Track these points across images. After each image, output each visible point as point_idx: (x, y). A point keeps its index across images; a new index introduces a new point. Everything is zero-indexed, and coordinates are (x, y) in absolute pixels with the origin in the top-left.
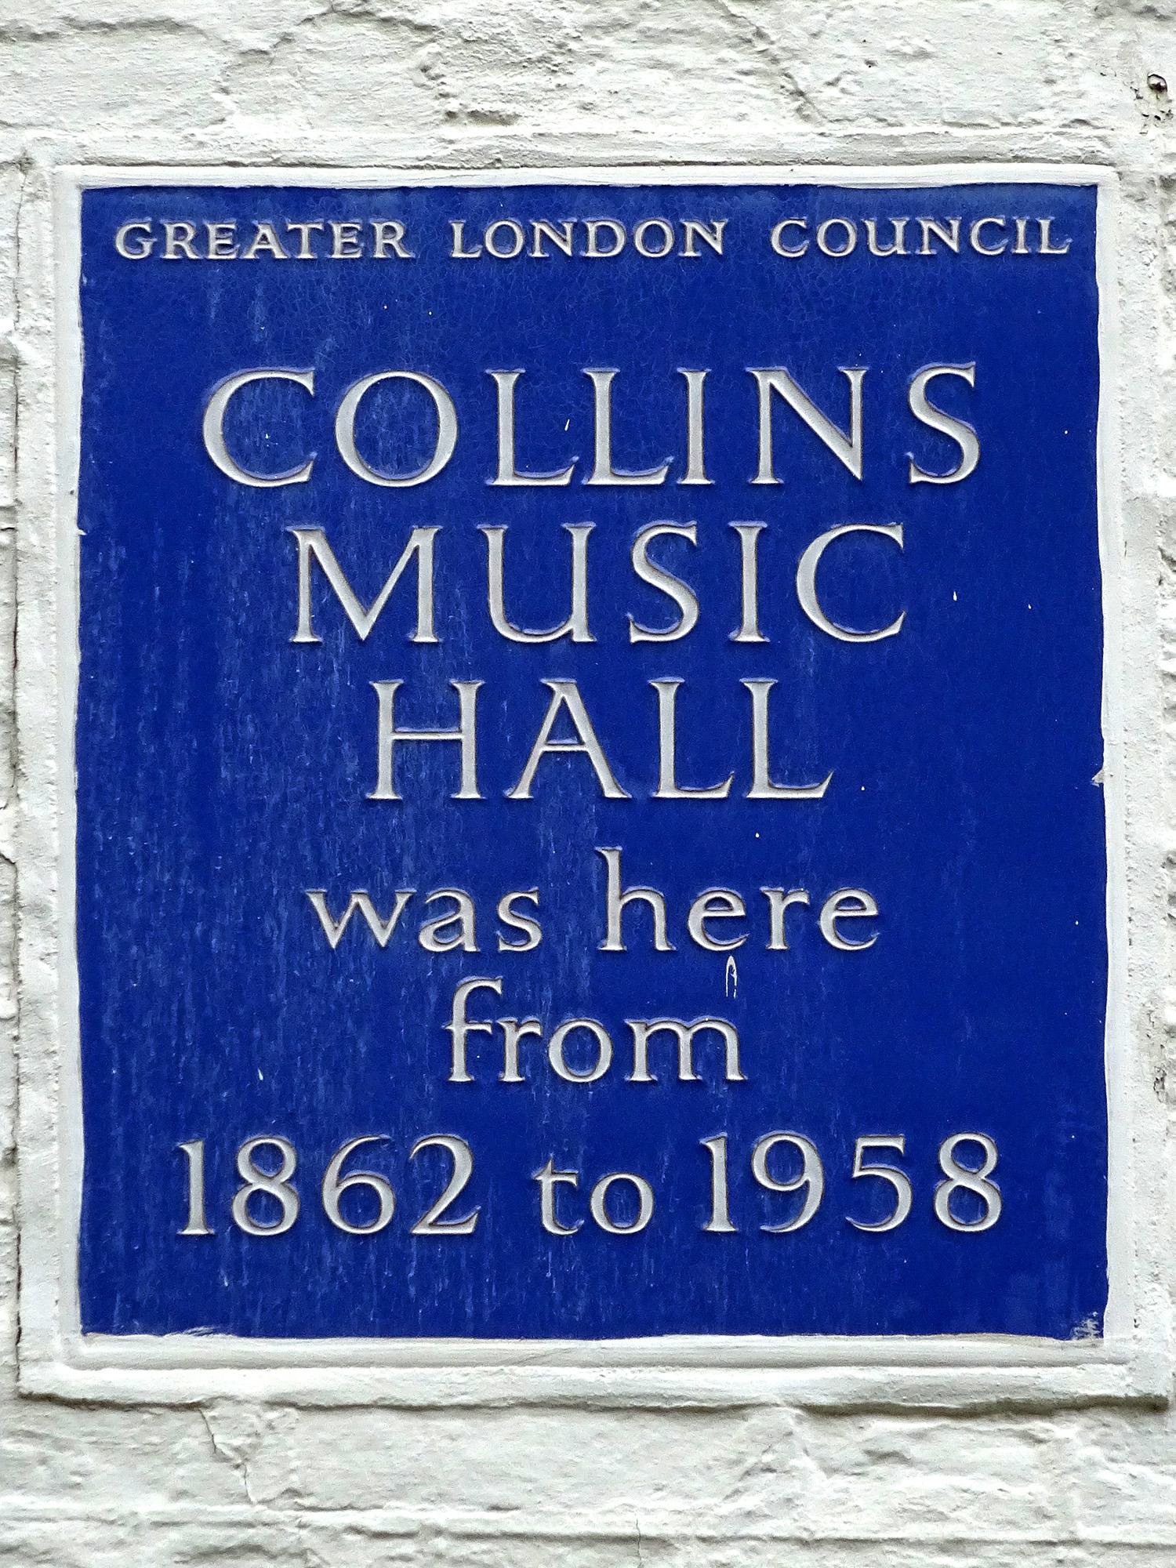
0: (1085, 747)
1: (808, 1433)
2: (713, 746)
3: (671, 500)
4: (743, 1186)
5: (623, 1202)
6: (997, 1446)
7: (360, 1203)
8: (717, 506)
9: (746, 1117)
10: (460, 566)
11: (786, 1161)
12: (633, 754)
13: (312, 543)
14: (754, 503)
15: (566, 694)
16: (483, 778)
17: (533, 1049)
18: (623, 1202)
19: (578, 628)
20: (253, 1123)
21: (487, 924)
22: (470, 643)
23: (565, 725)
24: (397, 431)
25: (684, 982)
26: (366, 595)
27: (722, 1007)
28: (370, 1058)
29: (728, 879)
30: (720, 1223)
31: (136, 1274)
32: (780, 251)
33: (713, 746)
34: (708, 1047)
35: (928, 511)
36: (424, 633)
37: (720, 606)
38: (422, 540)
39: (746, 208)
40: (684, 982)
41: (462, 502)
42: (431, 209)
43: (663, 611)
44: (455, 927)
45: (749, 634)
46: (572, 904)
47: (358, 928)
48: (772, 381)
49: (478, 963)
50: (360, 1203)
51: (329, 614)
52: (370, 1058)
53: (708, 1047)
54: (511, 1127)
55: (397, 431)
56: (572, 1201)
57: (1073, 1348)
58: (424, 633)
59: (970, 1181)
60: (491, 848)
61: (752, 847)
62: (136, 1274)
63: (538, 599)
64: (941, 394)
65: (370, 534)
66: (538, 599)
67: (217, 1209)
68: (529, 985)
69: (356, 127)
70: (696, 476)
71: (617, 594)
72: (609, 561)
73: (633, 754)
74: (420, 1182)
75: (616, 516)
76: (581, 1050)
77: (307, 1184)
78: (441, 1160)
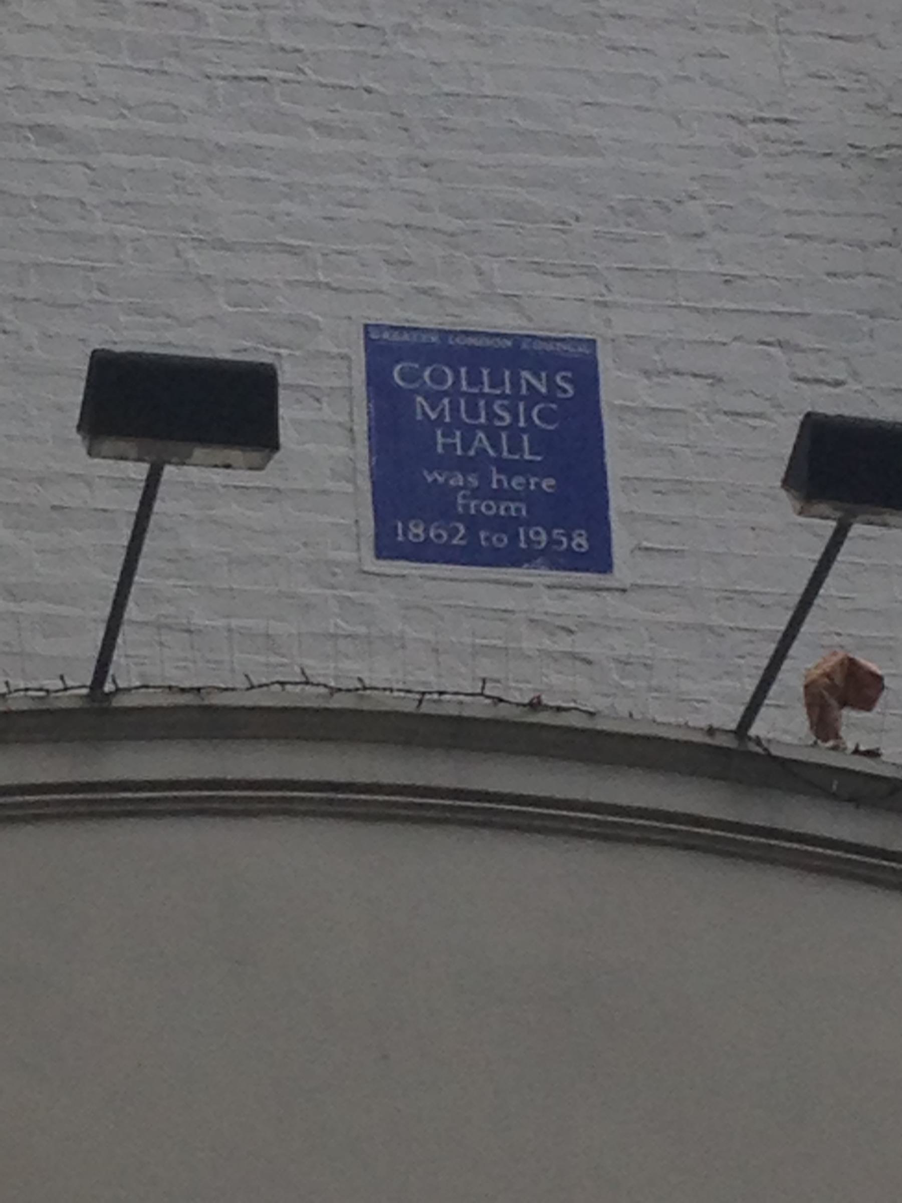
0: (601, 453)
1: (547, 591)
2: (515, 447)
3: (503, 396)
4: (528, 540)
5: (500, 540)
6: (588, 598)
7: (439, 536)
8: (516, 397)
9: (528, 524)
10: (454, 409)
11: (537, 533)
12: (496, 446)
13: (419, 399)
14: (523, 398)
15: (481, 435)
16: (463, 448)
17: (477, 508)
18: (500, 540)
19: (483, 420)
20: (413, 517)
21: (465, 480)
22: (457, 422)
23: (481, 441)
24: (438, 378)
25: (513, 496)
26: (433, 409)
27: (521, 500)
28: (441, 507)
29: (521, 474)
30: (523, 545)
31: (387, 548)
32: (467, 421)
33: (515, 447)
34: (518, 510)
35: (561, 402)
36: (447, 420)
37: (516, 418)
38: (446, 401)
39: (517, 339)
40: (513, 496)
41: (455, 393)
42: (444, 334)
43: (501, 418)
44: (458, 480)
45: (522, 424)
46: (485, 479)
47: (435, 480)
48: (526, 374)
49: (464, 488)
50: (439, 536)
51: (424, 413)
52: (441, 507)
53: (518, 510)
54: (474, 523)
55: (438, 378)
56: (487, 539)
57: (608, 576)
58: (447, 420)
59: (580, 541)
60: (465, 465)
61: (525, 469)
62: (387, 548)
63: (473, 412)
64: (564, 378)
65: (434, 399)
66: (473, 412)
67: (405, 534)
68: (475, 493)
69: (427, 317)
70: (508, 391)
71: (492, 415)
72: (489, 406)
73: (496, 446)
74: (453, 533)
75: (490, 400)
76: (489, 508)
77: (426, 530)
78: (457, 530)
